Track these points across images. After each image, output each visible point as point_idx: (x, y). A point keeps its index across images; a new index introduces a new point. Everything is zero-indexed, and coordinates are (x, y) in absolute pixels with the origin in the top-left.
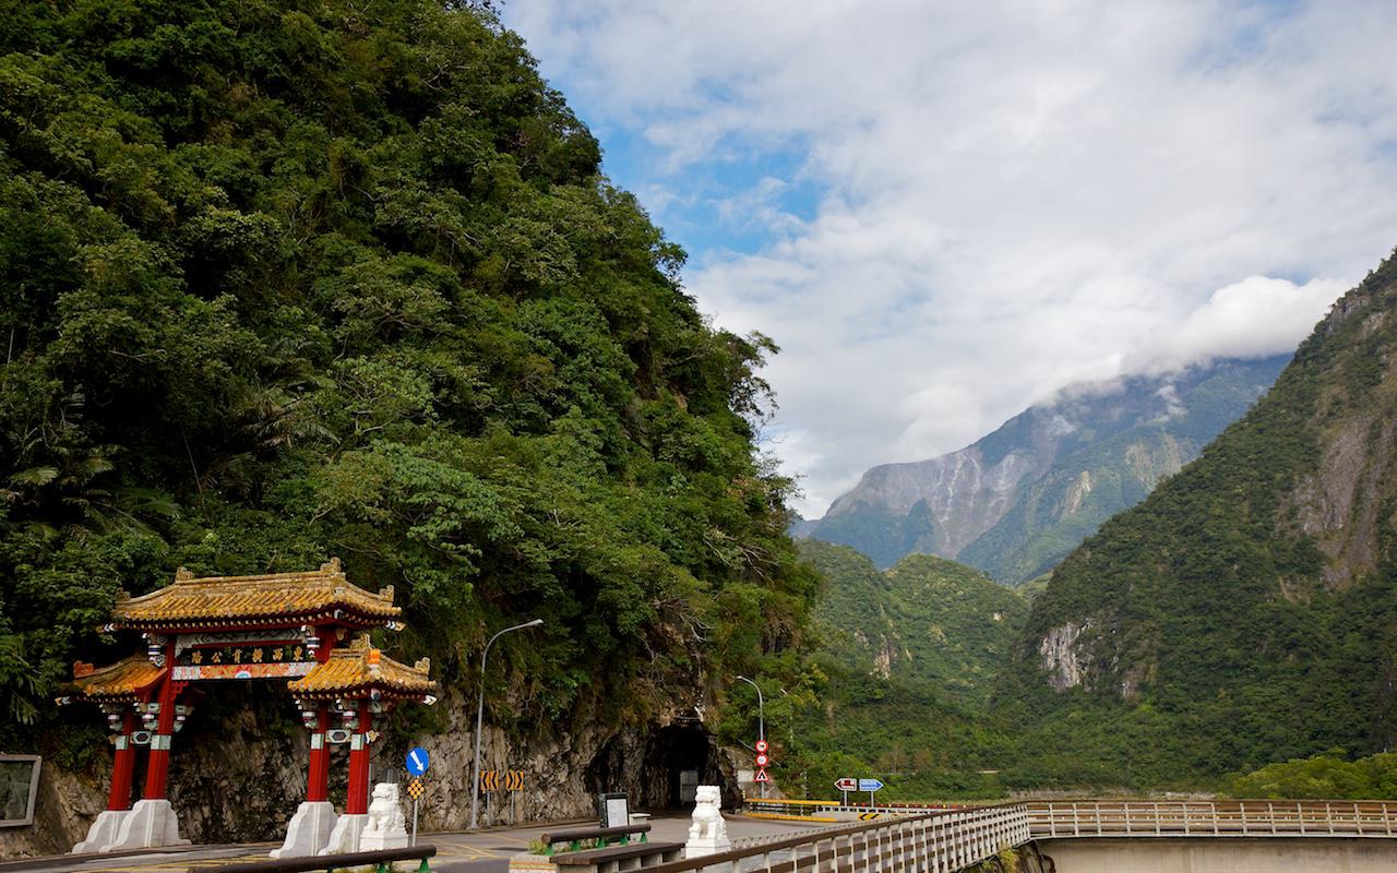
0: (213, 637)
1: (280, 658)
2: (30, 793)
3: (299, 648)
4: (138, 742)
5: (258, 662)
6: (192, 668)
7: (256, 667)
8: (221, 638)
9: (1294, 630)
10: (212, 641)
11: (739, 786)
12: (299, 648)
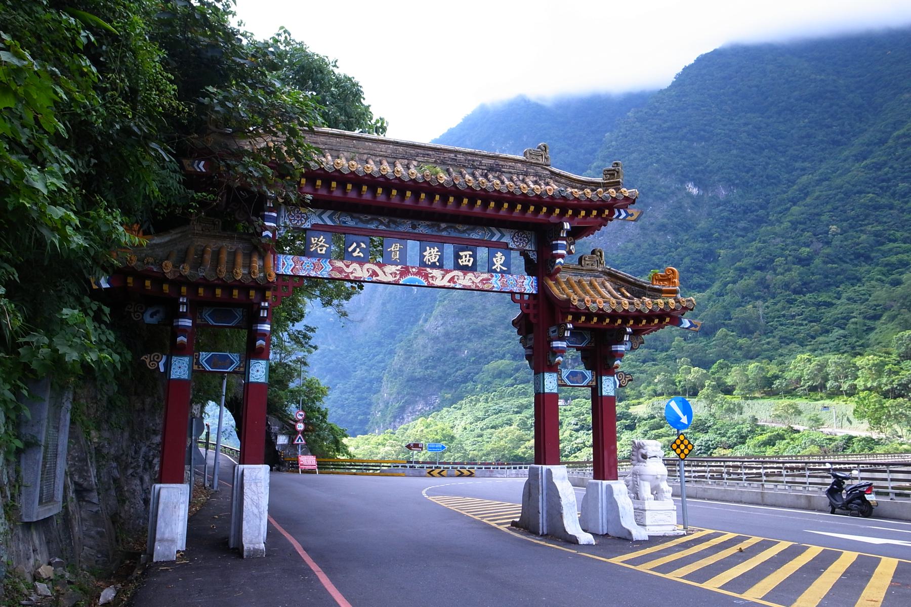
0: (353, 218)
1: (470, 265)
2: (60, 448)
3: (499, 254)
4: (208, 368)
5: (433, 266)
6: (315, 260)
7: (436, 273)
8: (367, 222)
9: (332, 362)
10: (351, 223)
11: (277, 448)
12: (499, 254)
